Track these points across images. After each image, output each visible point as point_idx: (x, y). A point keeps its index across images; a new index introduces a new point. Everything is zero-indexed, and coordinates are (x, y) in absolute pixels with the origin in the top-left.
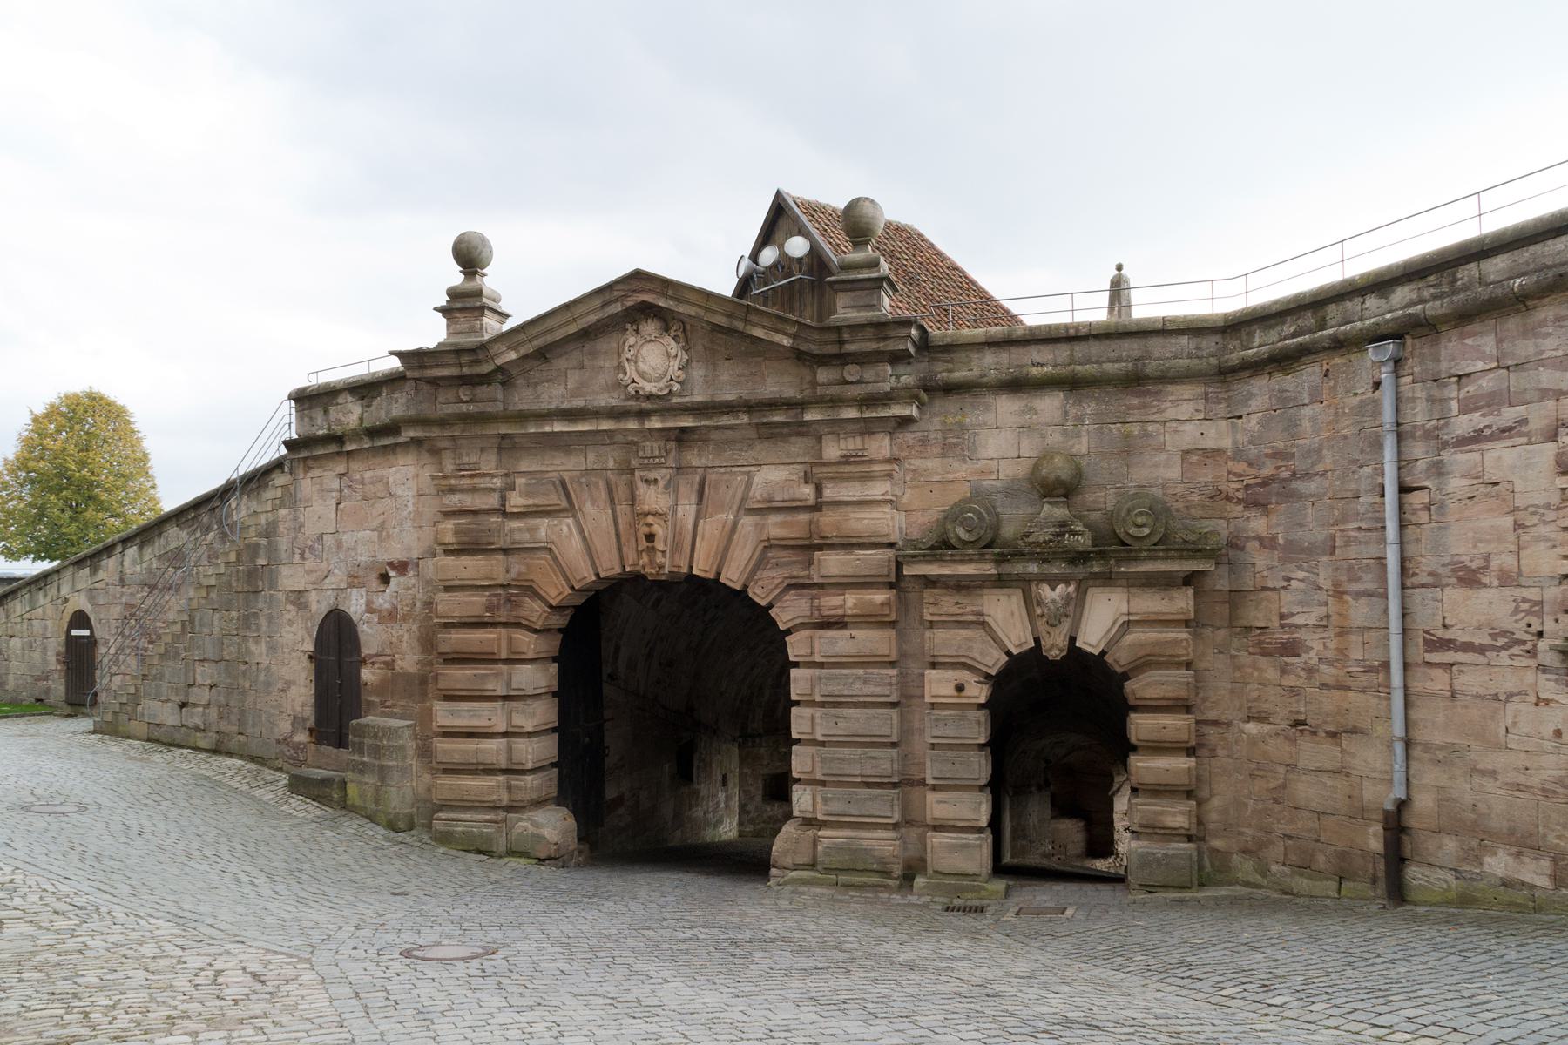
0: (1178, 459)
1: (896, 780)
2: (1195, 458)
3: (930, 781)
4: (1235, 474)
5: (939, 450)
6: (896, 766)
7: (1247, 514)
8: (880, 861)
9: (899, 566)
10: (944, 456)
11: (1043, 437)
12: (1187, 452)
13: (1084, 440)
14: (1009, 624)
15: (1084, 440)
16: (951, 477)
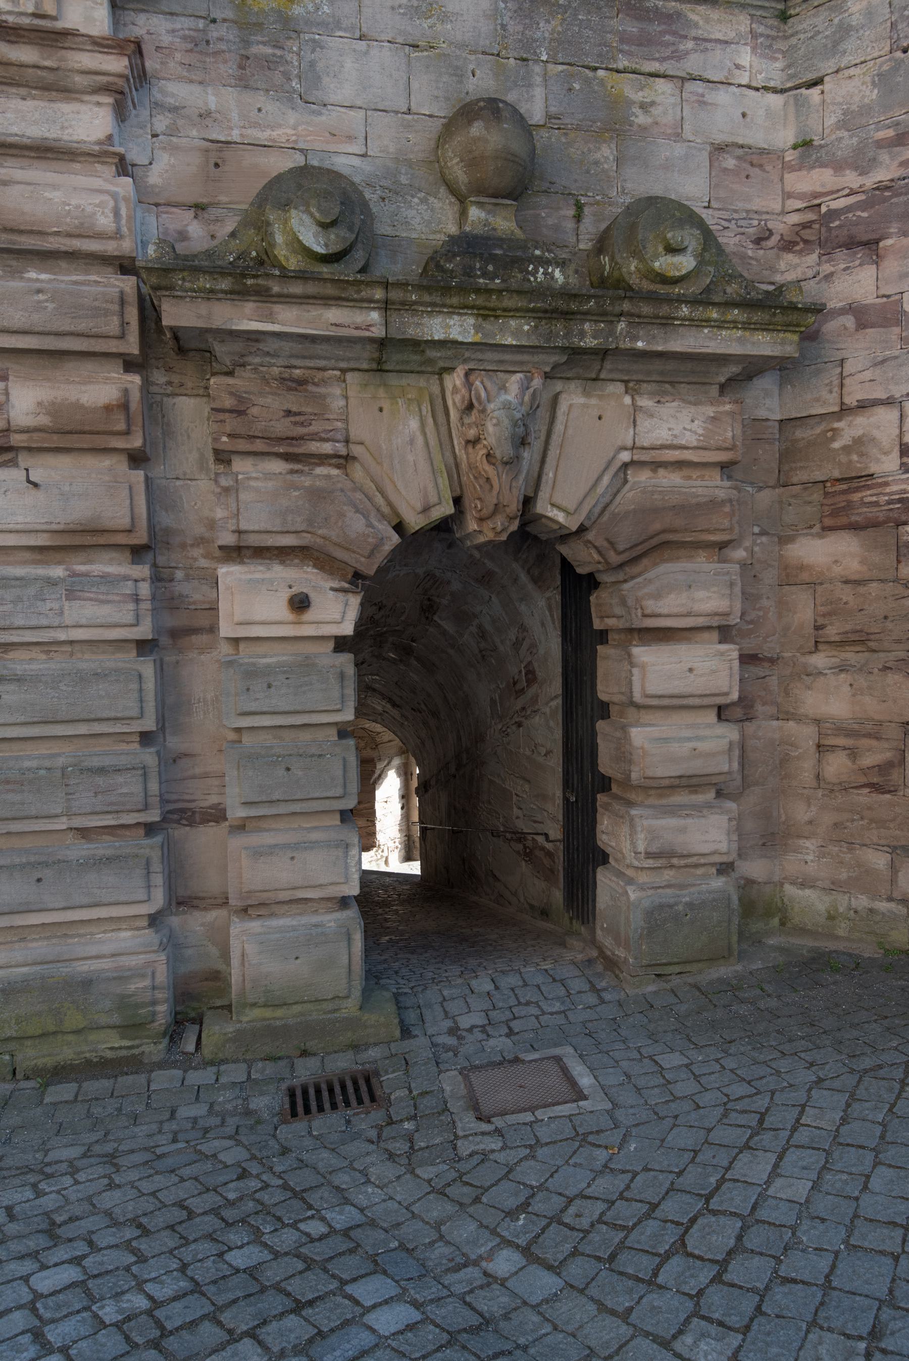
0: (703, 157)
1: (154, 816)
2: (730, 162)
3: (236, 812)
4: (801, 196)
5: (228, 68)
6: (154, 787)
7: (827, 268)
8: (124, 1003)
9: (149, 314)
10: (244, 84)
11: (459, 74)
12: (720, 149)
13: (539, 93)
14: (402, 457)
15: (539, 93)
16: (263, 136)
